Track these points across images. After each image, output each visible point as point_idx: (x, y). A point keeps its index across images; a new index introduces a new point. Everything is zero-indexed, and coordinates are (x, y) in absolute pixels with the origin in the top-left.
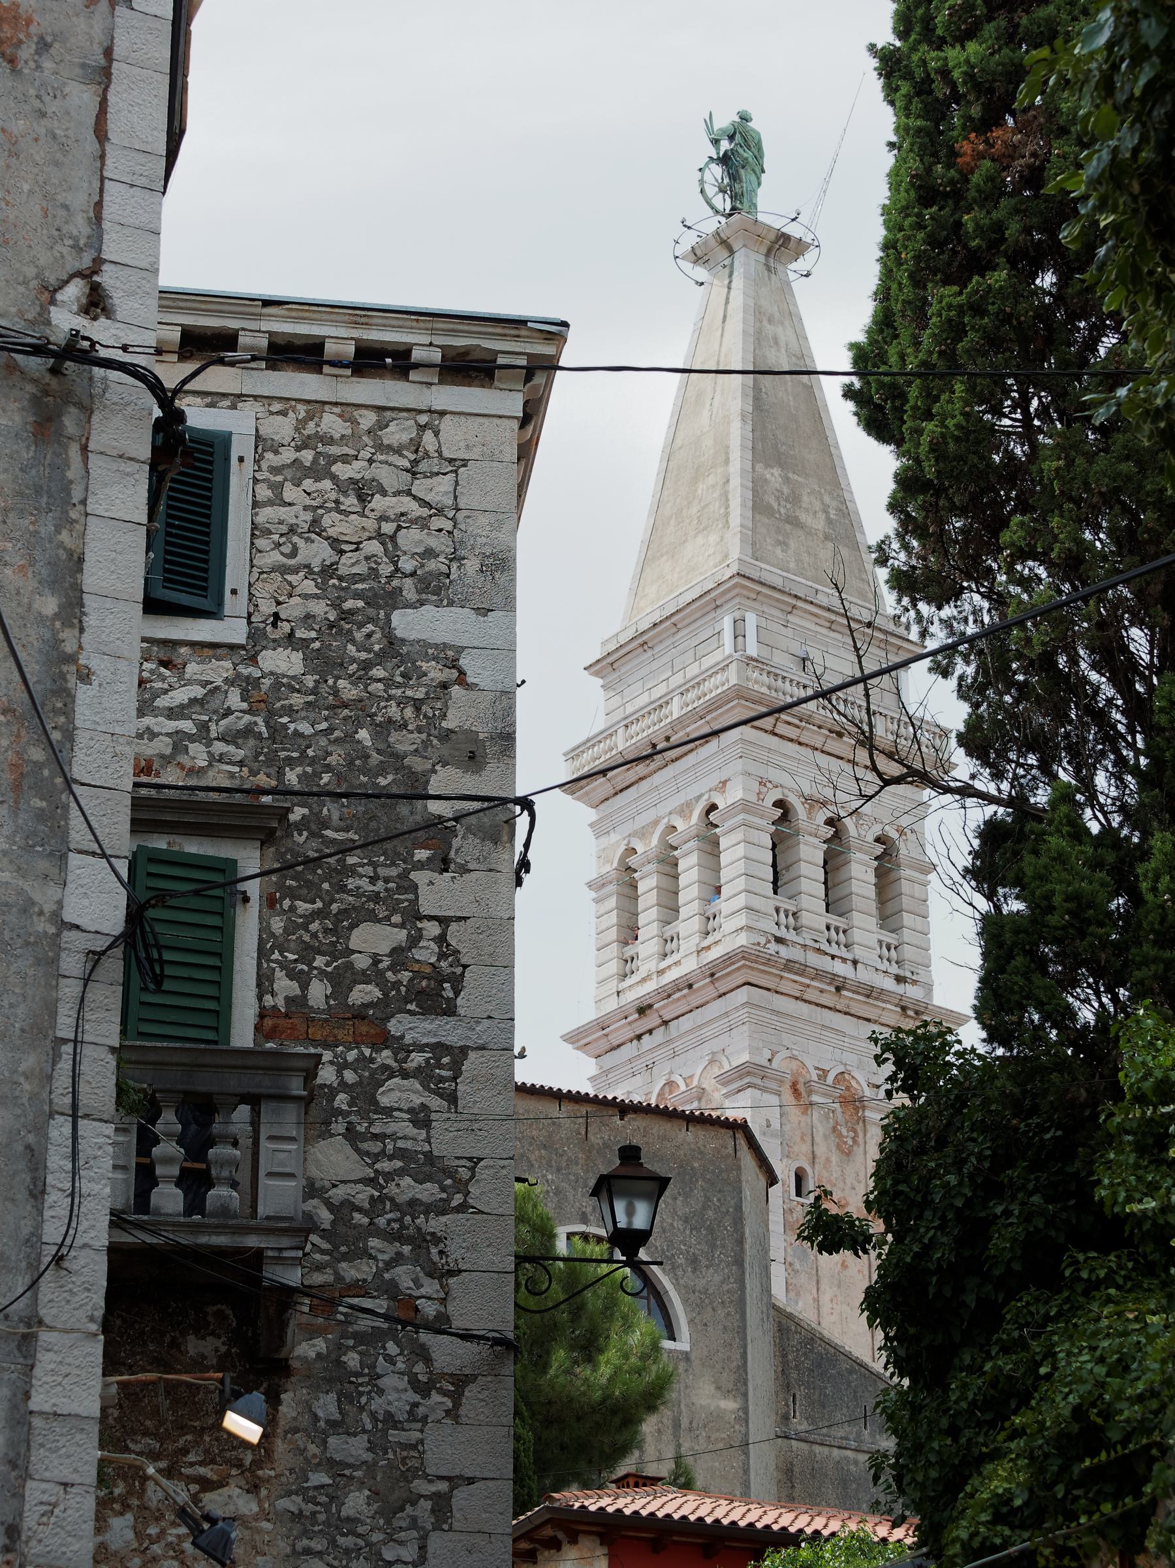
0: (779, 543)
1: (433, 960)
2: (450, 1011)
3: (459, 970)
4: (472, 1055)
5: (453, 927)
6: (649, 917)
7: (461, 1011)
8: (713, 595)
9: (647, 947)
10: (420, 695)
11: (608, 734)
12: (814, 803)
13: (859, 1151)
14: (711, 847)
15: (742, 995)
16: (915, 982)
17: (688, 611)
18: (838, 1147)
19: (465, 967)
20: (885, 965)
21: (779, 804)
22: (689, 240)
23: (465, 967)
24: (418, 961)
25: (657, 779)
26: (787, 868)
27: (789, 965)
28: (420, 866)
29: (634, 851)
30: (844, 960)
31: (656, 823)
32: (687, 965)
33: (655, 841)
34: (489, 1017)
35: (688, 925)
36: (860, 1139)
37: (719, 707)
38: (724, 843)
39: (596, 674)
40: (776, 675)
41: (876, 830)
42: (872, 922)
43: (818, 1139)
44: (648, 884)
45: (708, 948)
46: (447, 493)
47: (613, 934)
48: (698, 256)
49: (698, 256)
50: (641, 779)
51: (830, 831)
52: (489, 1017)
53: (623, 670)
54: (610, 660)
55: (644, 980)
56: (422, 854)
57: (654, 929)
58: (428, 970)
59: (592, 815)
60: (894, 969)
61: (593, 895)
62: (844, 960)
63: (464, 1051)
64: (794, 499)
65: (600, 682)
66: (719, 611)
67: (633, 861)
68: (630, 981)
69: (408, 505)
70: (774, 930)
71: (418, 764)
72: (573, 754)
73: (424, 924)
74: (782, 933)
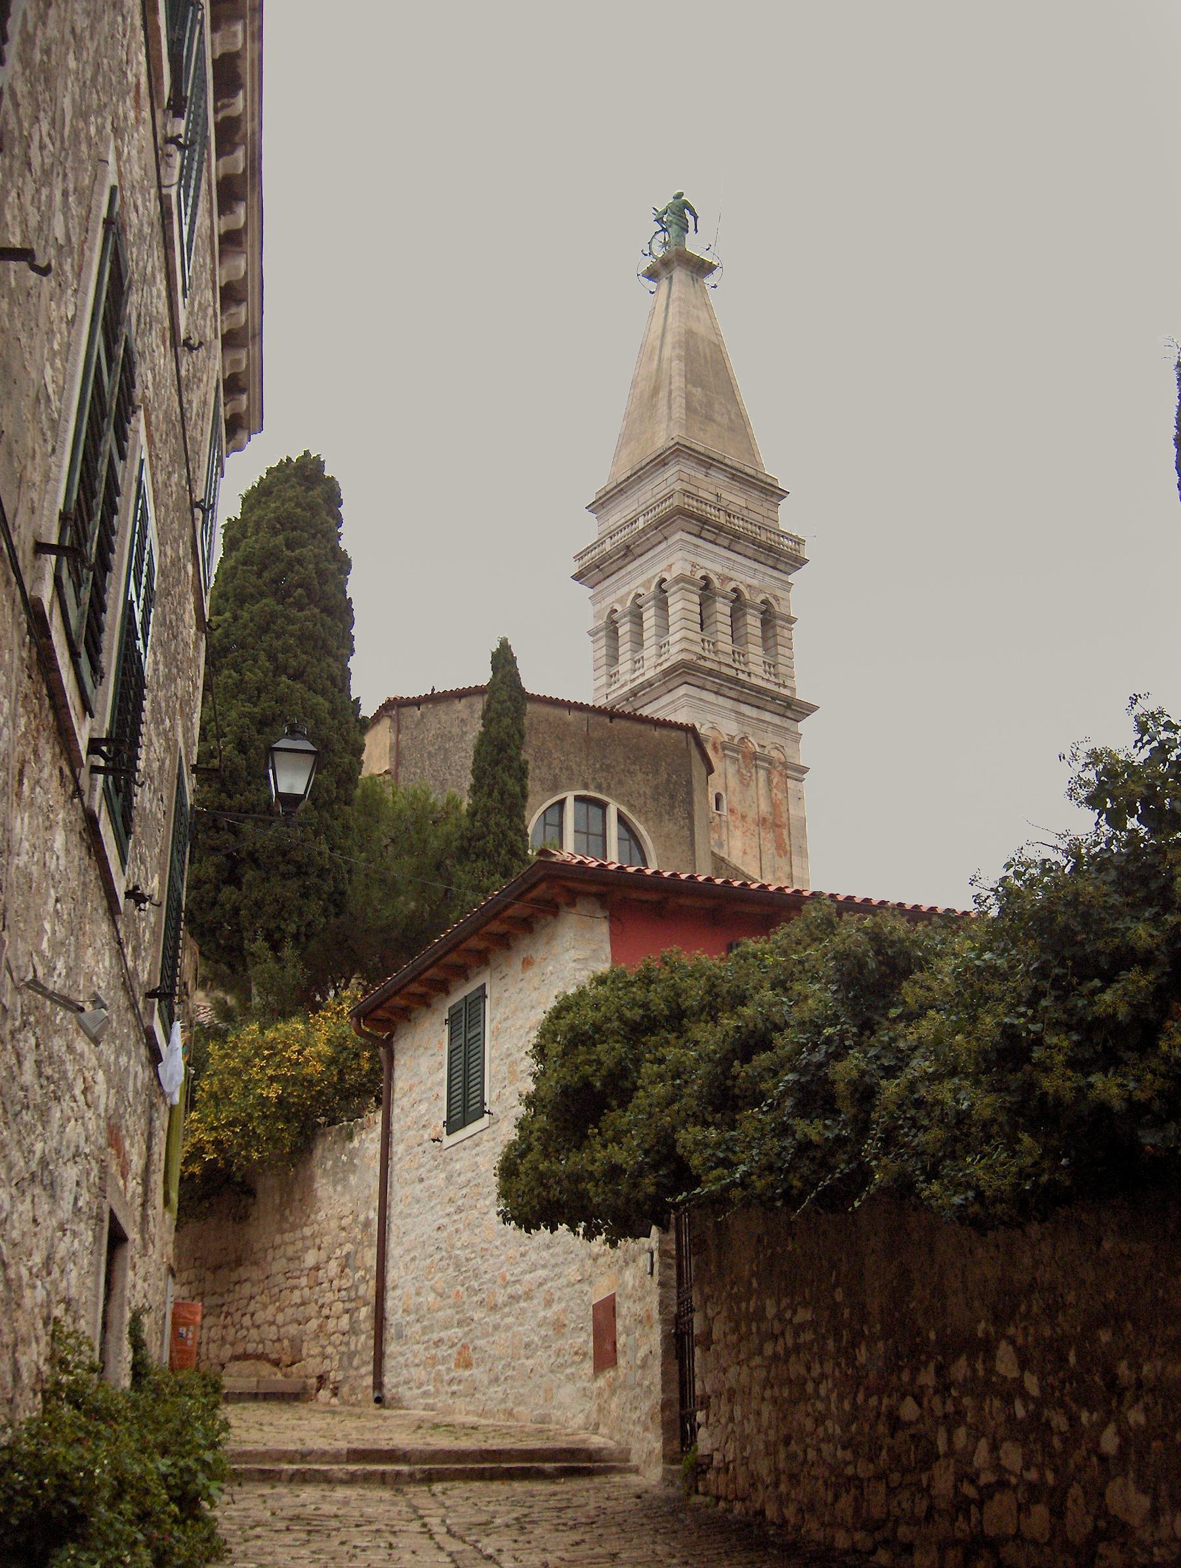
0: (701, 429)
6: (625, 649)
9: (624, 666)
11: (600, 542)
12: (726, 579)
13: (753, 784)
14: (663, 605)
15: (684, 690)
16: (785, 687)
18: (742, 783)
20: (767, 676)
21: (704, 578)
25: (629, 568)
26: (708, 617)
27: (710, 672)
30: (743, 672)
31: (629, 593)
32: (650, 673)
33: (629, 603)
35: (649, 651)
36: (754, 777)
38: (670, 601)
41: (762, 597)
42: (760, 651)
43: (730, 776)
44: (624, 629)
45: (661, 664)
47: (604, 661)
48: (652, 275)
49: (652, 275)
51: (734, 596)
55: (622, 686)
57: (628, 655)
59: (591, 592)
60: (773, 678)
62: (743, 672)
64: (710, 405)
67: (615, 616)
68: (613, 688)
70: (702, 652)
72: (579, 557)
74: (706, 654)
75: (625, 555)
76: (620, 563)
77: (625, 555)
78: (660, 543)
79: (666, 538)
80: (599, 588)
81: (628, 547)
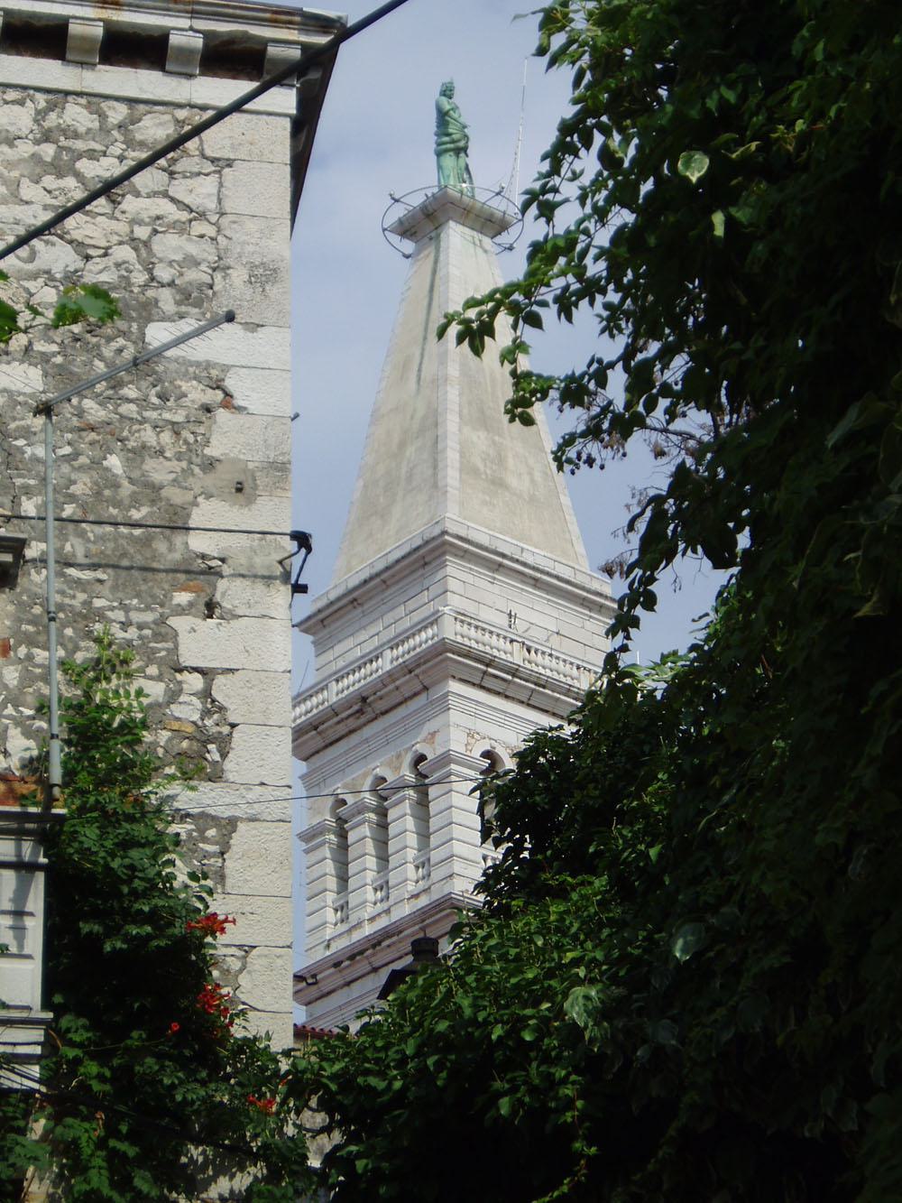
1: (196, 717)
2: (216, 776)
3: (226, 730)
4: (241, 826)
5: (220, 681)
7: (230, 776)
8: (422, 552)
10: (179, 417)
11: (321, 687)
17: (398, 567)
19: (233, 726)
21: (488, 754)
22: (399, 212)
23: (233, 726)
24: (178, 719)
25: (367, 732)
28: (181, 611)
29: (344, 802)
34: (263, 784)
37: (428, 661)
39: (306, 631)
40: (484, 629)
46: (209, 195)
50: (351, 732)
52: (263, 784)
53: (333, 626)
54: (321, 616)
56: (182, 598)
58: (190, 729)
61: (304, 846)
63: (232, 823)
64: (500, 460)
65: (311, 638)
66: (427, 568)
69: (165, 207)
71: (176, 496)
73: (185, 676)
75: (360, 712)
76: (352, 723)
77: (360, 712)
78: (416, 694)
79: (426, 688)
80: (317, 761)
81: (364, 699)
